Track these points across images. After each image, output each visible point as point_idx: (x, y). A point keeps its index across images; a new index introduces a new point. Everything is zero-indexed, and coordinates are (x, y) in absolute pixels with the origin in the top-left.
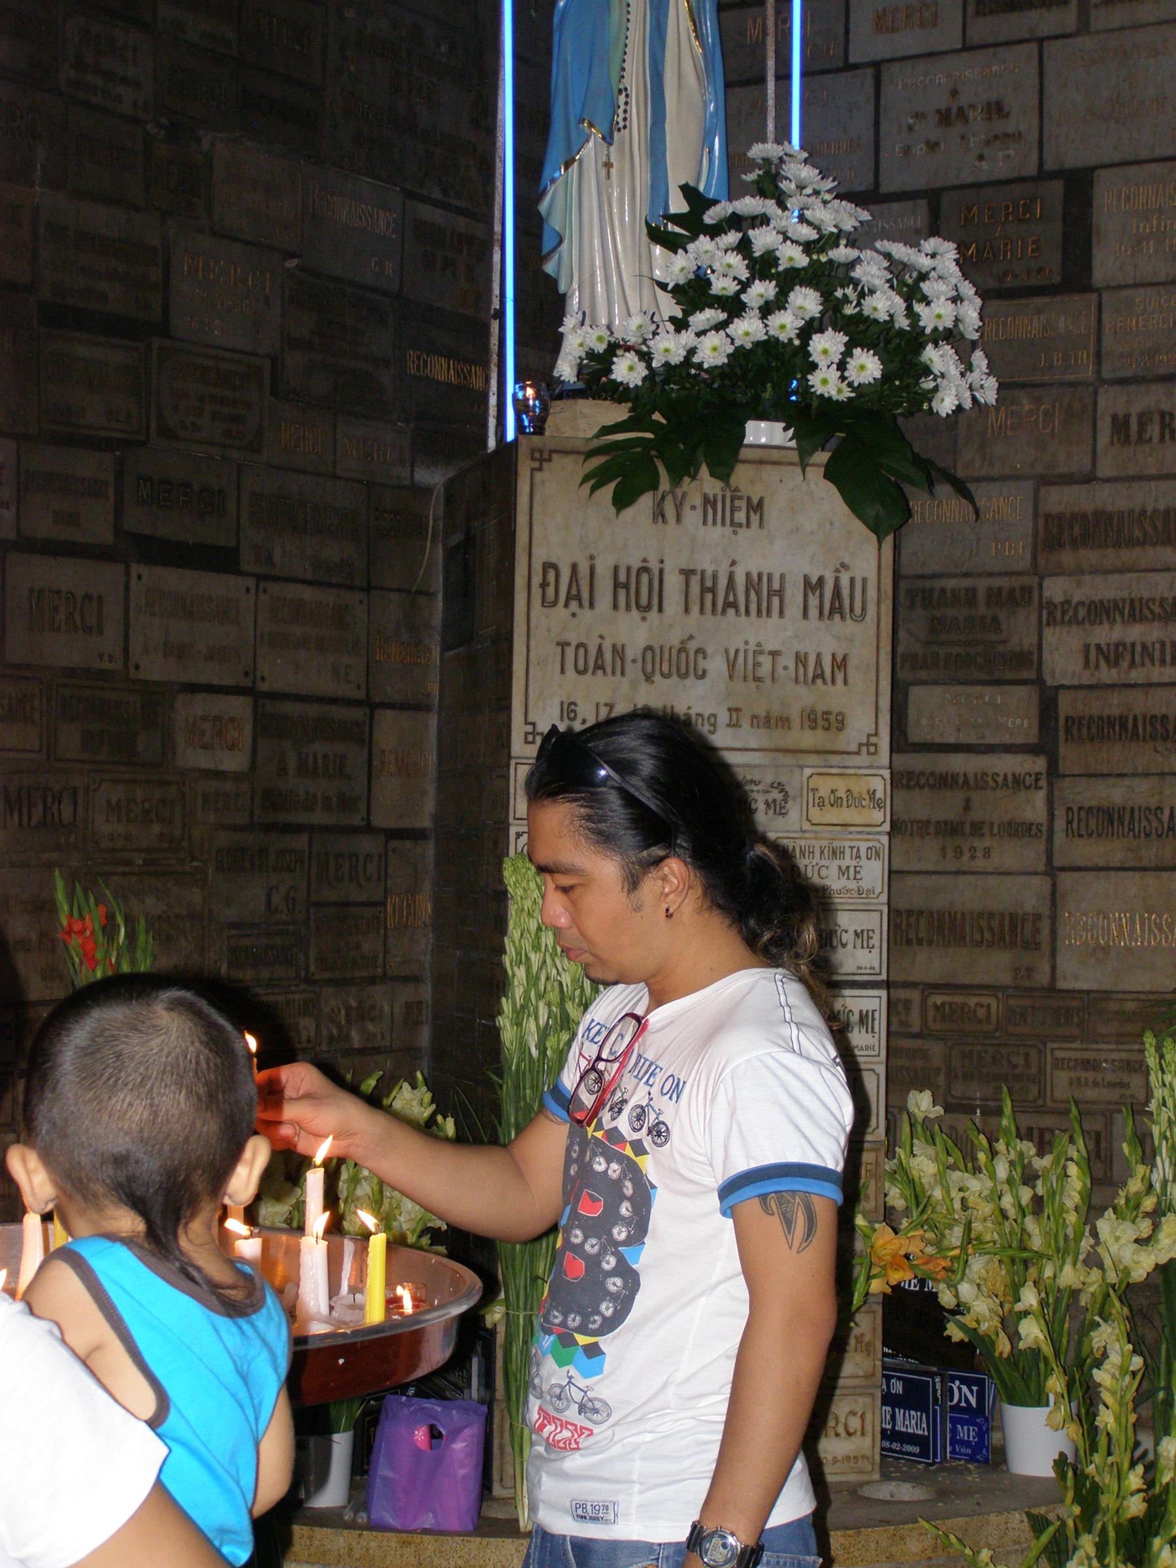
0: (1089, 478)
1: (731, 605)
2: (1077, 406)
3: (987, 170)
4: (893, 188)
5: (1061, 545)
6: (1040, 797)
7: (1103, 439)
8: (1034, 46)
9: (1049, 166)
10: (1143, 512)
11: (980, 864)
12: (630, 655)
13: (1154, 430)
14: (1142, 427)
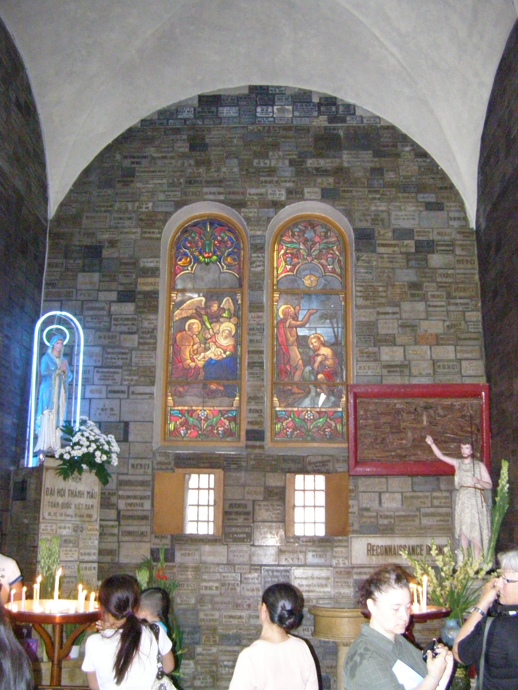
0: (127, 474)
1: (76, 496)
3: (110, 420)
6: (117, 529)
9: (122, 420)
11: (105, 540)
13: (139, 467)
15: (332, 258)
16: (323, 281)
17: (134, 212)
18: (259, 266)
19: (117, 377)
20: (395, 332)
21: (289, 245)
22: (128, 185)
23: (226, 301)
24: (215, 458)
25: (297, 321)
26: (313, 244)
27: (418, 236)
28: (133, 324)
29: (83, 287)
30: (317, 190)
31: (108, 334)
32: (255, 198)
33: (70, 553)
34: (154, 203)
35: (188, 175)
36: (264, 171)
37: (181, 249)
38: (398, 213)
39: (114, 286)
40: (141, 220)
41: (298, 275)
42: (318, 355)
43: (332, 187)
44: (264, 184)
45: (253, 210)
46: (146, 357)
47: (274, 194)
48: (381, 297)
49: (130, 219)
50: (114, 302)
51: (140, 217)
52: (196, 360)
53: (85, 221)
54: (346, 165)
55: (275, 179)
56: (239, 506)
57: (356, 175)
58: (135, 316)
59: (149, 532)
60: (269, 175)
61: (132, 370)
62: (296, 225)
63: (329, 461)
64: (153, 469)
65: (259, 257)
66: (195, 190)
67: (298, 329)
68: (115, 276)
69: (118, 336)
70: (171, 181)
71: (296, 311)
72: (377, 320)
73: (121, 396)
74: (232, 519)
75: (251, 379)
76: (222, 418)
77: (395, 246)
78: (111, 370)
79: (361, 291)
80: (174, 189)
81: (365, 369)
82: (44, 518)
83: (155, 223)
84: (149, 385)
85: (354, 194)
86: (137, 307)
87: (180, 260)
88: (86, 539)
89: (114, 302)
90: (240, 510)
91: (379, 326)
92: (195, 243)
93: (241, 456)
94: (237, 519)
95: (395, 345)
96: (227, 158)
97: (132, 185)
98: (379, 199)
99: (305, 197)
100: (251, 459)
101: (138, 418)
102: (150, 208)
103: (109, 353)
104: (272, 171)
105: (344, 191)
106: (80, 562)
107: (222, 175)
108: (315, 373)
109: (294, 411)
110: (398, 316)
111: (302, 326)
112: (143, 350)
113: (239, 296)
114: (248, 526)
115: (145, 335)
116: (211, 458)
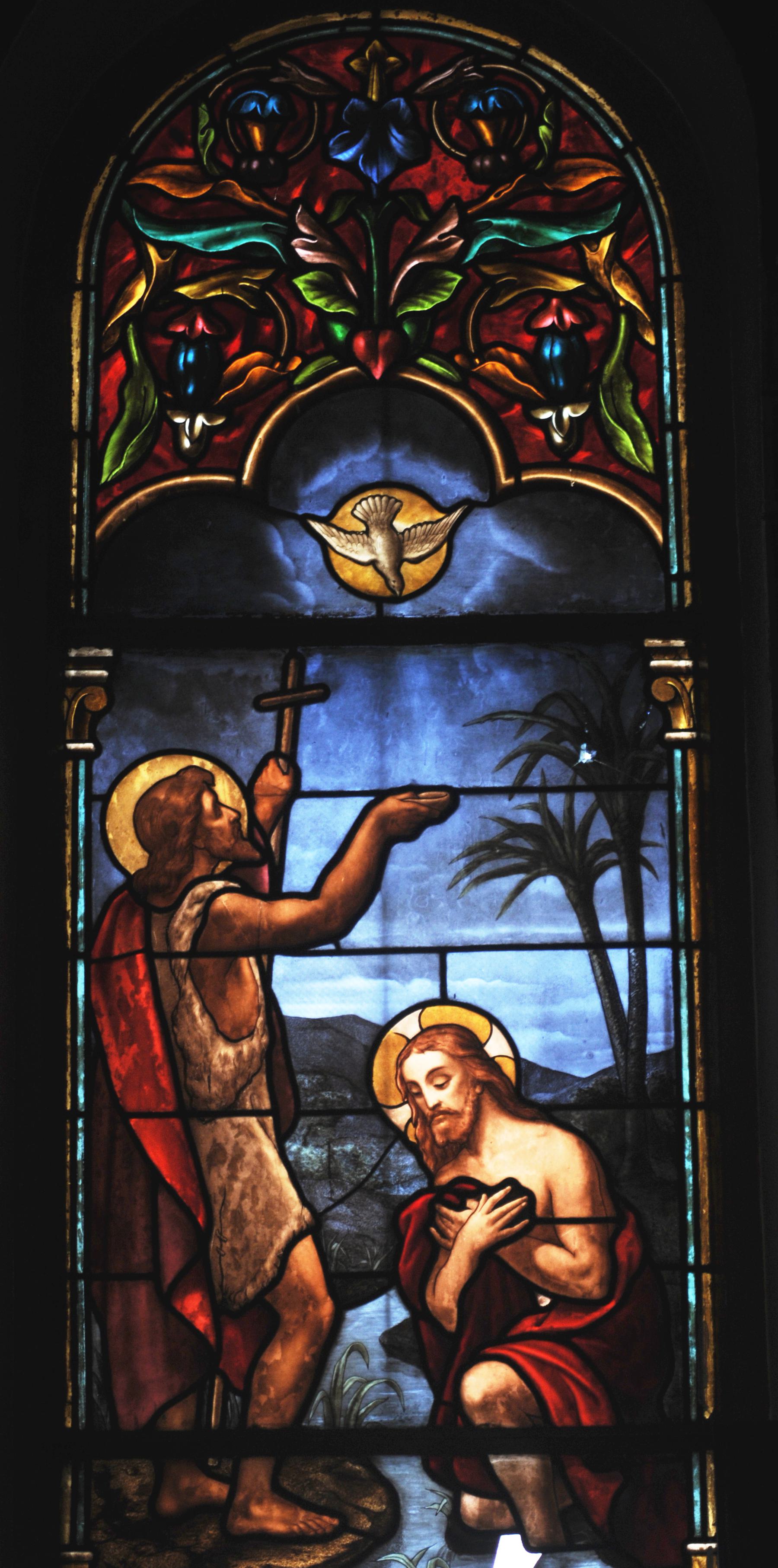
67: (282, 965)
71: (264, 809)
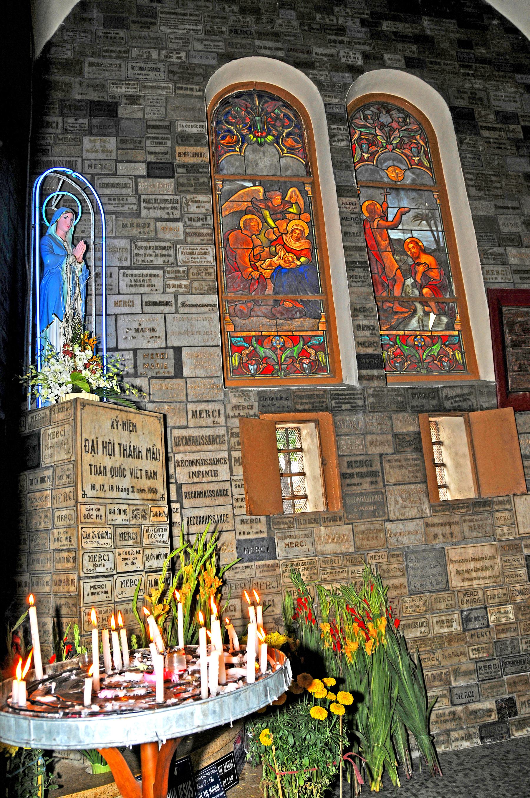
0: (187, 427)
2: (181, 408)
4: (123, 347)
5: (180, 445)
7: (190, 416)
8: (163, 315)
9: (169, 345)
10: (203, 436)
12: (108, 469)
13: (204, 415)
14: (200, 414)
15: (417, 148)
16: (410, 174)
17: (160, 61)
18: (342, 140)
19: (158, 283)
20: (520, 230)
21: (362, 130)
22: (148, 28)
23: (292, 193)
24: (318, 396)
25: (387, 221)
26: (390, 130)
27: (524, 121)
28: (173, 208)
29: (92, 156)
30: (399, 57)
31: (136, 221)
32: (325, 59)
33: (131, 557)
34: (188, 52)
35: (231, 23)
36: (330, 29)
37: (222, 124)
38: (497, 94)
39: (139, 155)
40: (172, 72)
41: (379, 166)
42: (419, 264)
43: (415, 56)
44: (333, 44)
45: (324, 73)
46: (199, 254)
47: (348, 56)
48: (497, 188)
49: (156, 69)
50: (143, 177)
51: (171, 68)
52: (259, 268)
53: (87, 69)
54: (428, 32)
55: (346, 39)
56: (362, 463)
57: (442, 46)
58: (178, 197)
59: (231, 515)
60: (337, 34)
61: (178, 272)
62: (367, 107)
63: (469, 394)
64: (227, 417)
65: (340, 129)
66: (244, 42)
67: (390, 231)
68: (140, 142)
69: (152, 224)
70: (208, 28)
72: (496, 214)
73: (167, 309)
74: (354, 485)
75: (354, 284)
76: (306, 347)
77: (501, 130)
78: (145, 272)
79: (471, 180)
80: (213, 37)
81: (493, 274)
82: (84, 495)
83: (193, 78)
84: (208, 293)
85: (444, 67)
86: (178, 185)
87: (223, 138)
88: (151, 531)
89: (143, 177)
90: (364, 470)
91: (500, 222)
92: (241, 118)
93: (355, 392)
94: (361, 484)
95: (522, 246)
96: (280, 8)
97: (154, 28)
98: (473, 75)
99: (387, 65)
100: (369, 396)
101: (197, 340)
102: (184, 59)
103: (140, 248)
104: (341, 30)
105: (431, 63)
106: (147, 572)
107: (277, 29)
108: (419, 286)
109: (399, 335)
110: (518, 211)
111: (395, 227)
112: (192, 243)
113: (308, 188)
114: (378, 493)
115: (194, 223)
116: (312, 396)
